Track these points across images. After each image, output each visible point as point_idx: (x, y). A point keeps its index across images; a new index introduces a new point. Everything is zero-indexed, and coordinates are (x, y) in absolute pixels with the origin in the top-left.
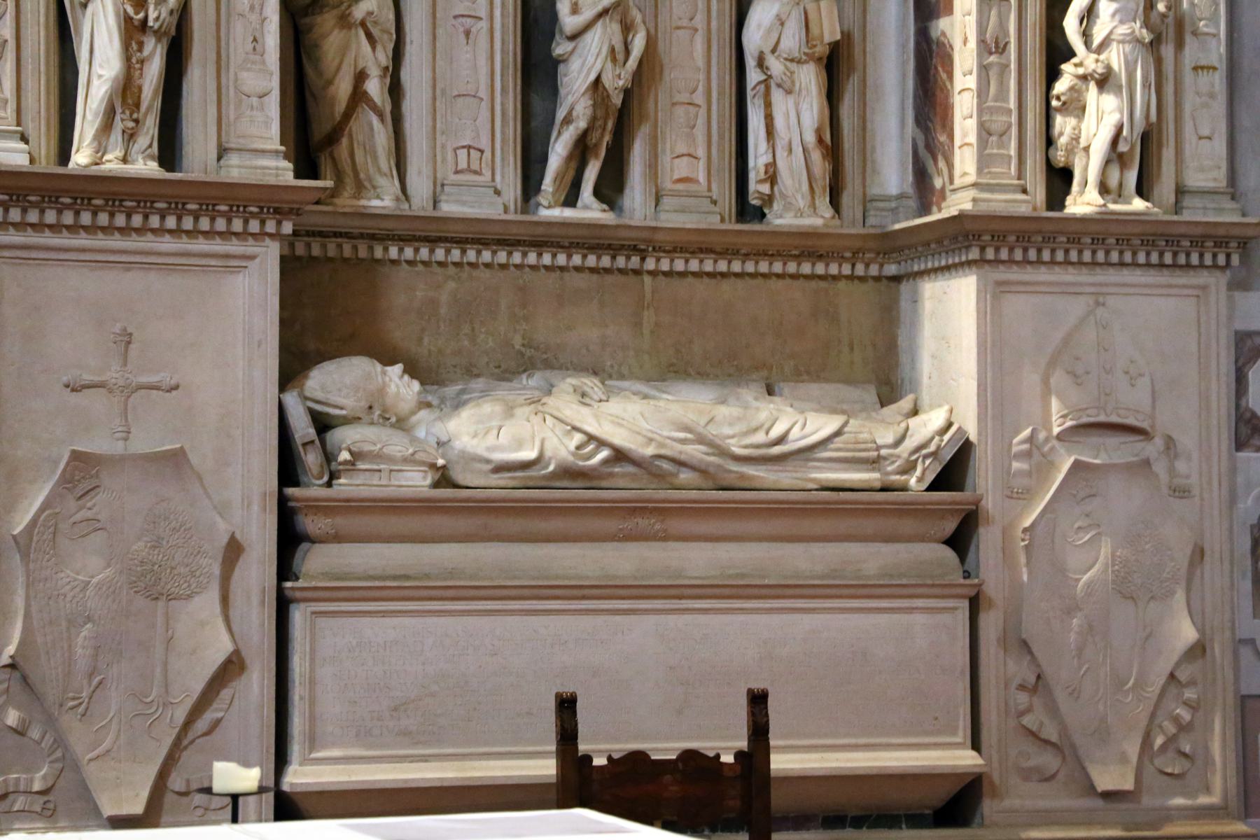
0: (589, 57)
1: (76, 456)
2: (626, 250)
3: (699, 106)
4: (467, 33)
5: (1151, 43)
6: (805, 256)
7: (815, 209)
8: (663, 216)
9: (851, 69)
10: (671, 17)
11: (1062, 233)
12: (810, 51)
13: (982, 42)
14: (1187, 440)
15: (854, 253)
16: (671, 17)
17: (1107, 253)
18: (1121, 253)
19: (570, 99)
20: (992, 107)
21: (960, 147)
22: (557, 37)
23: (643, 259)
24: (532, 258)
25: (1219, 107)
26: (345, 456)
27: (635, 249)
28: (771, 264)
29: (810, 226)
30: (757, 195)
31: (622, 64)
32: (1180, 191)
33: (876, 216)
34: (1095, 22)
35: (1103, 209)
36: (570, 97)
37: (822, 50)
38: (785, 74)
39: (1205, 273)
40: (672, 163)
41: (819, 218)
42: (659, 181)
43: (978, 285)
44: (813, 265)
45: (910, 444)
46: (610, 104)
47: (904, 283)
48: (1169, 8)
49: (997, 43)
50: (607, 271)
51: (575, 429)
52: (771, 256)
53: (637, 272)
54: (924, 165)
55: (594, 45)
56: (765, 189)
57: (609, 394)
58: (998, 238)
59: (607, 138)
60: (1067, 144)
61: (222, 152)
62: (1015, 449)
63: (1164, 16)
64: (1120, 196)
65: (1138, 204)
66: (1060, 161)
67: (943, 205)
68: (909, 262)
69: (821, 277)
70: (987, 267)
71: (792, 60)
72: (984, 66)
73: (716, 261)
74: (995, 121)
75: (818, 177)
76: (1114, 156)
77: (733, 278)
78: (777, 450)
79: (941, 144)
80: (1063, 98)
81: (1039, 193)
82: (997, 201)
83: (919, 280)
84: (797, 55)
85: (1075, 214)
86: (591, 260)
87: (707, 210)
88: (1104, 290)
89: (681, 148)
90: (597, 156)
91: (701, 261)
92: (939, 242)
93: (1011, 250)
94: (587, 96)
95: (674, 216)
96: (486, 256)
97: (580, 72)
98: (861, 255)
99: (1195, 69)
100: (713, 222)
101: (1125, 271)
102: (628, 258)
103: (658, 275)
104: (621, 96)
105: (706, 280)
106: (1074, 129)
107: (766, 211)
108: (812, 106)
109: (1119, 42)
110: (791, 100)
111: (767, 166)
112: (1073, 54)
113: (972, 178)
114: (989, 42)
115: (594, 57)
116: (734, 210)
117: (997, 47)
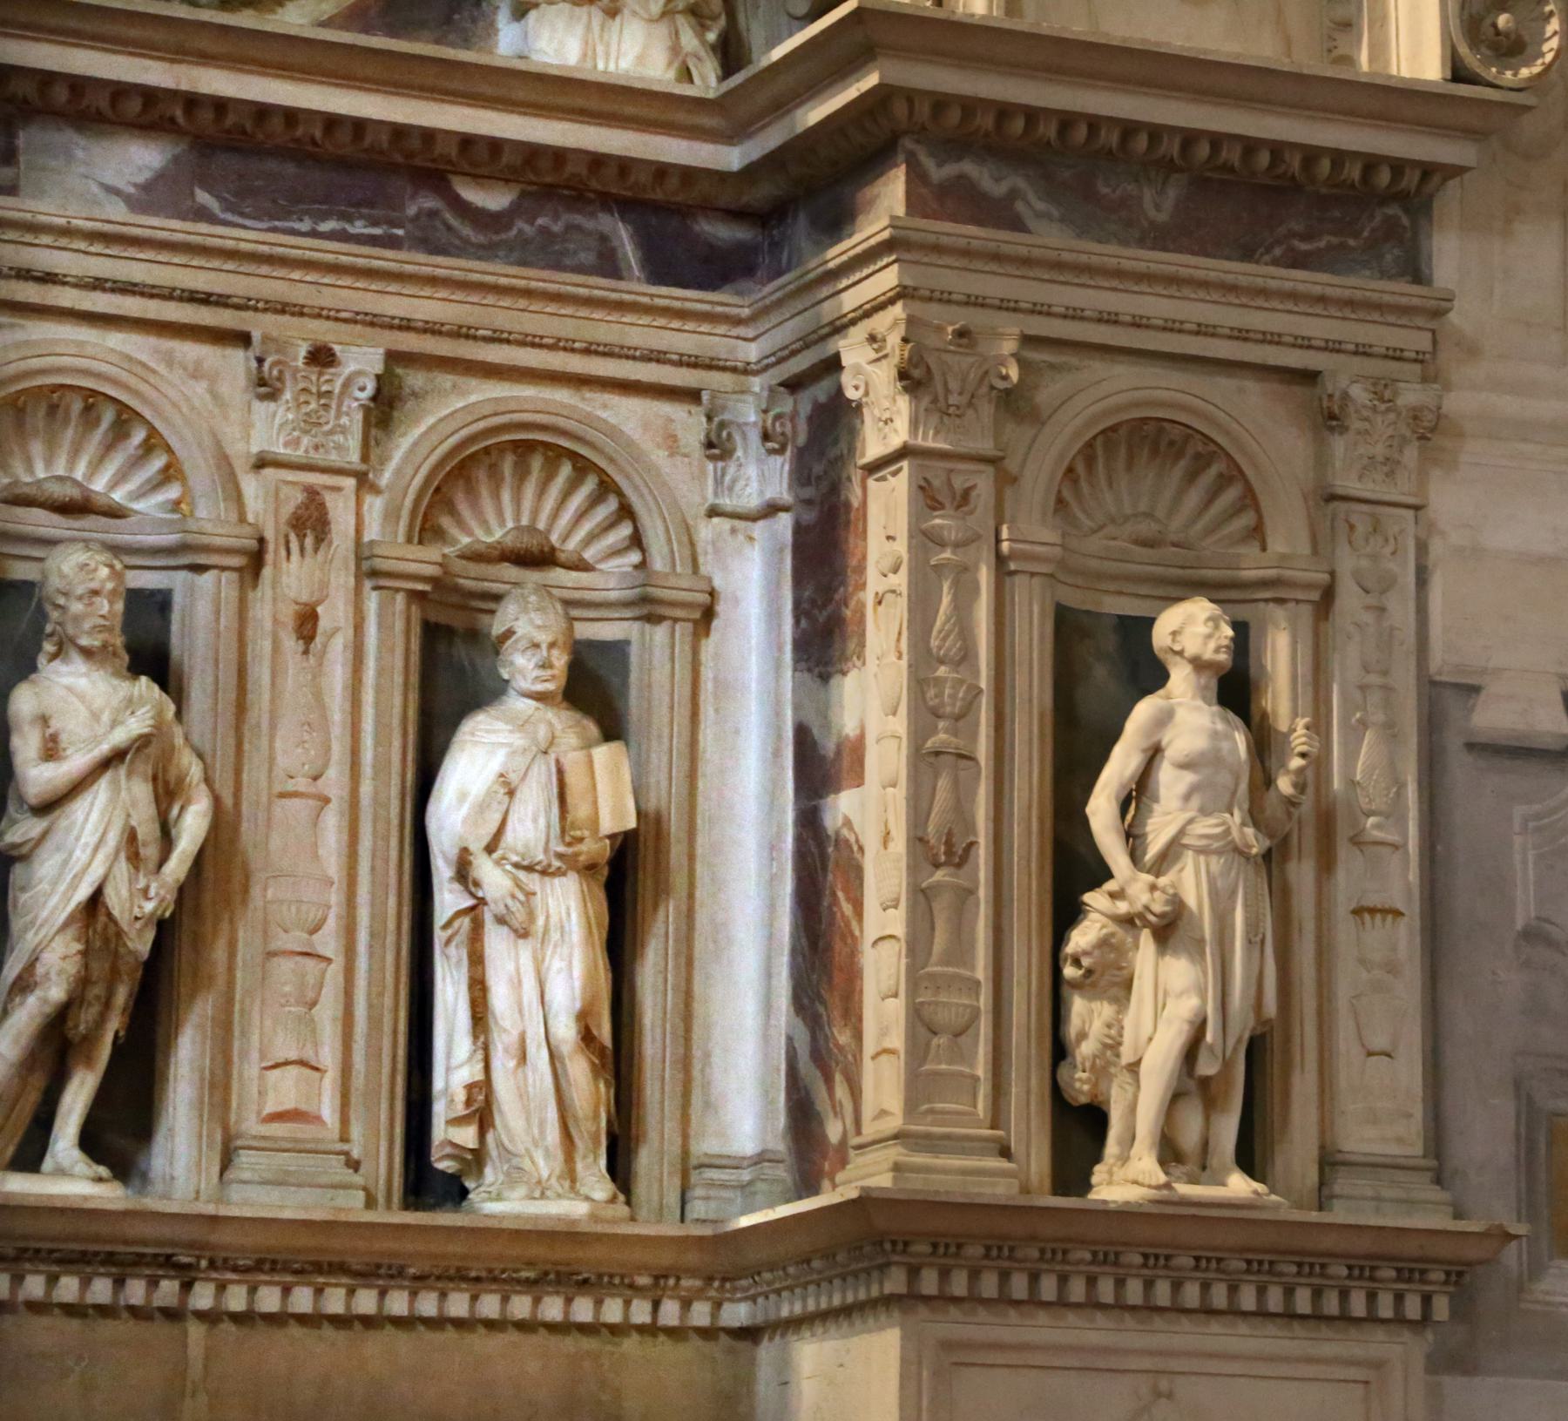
0: (78, 853)
2: (148, 1265)
3: (329, 960)
5: (1267, 856)
6: (550, 1283)
7: (573, 1180)
8: (236, 1193)
9: (662, 890)
10: (270, 770)
11: (1082, 1242)
12: (570, 850)
13: (917, 840)
15: (657, 1278)
16: (270, 770)
17: (1177, 1286)
18: (1206, 1287)
20: (943, 975)
21: (873, 1058)
22: (11, 808)
23: (187, 1286)
25: (1408, 990)
27: (168, 1263)
28: (474, 1298)
29: (559, 1219)
30: (448, 1150)
31: (152, 865)
32: (1329, 1161)
33: (707, 1198)
34: (1151, 811)
35: (1165, 1192)
36: (30, 935)
37: (595, 849)
38: (513, 897)
40: (261, 1078)
42: (233, 1118)
43: (903, 1348)
44: (569, 1301)
46: (122, 950)
47: (765, 1342)
48: (1300, 787)
49: (949, 844)
50: (104, 1311)
52: (476, 1283)
53: (173, 1315)
54: (808, 1093)
55: (89, 826)
56: (467, 1136)
58: (947, 1249)
59: (114, 1024)
60: (1095, 1057)
63: (1291, 803)
64: (1204, 1168)
65: (1239, 1185)
66: (1081, 1092)
67: (840, 1177)
68: (773, 1297)
69: (583, 1328)
70: (923, 1311)
71: (529, 869)
72: (923, 891)
73: (351, 1292)
74: (945, 1004)
75: (580, 1114)
76: (1192, 1085)
77: (389, 1329)
79: (841, 1048)
80: (1086, 962)
81: (1037, 1159)
82: (945, 1171)
83: (791, 1337)
84: (541, 857)
85: (1105, 1202)
87: (337, 1179)
88: (1174, 1364)
89: (286, 1048)
90: (89, 1062)
91: (319, 1291)
92: (829, 1255)
93: (975, 1274)
94: (71, 932)
95: (254, 1193)
97: (55, 883)
98: (671, 1282)
99: (1358, 912)
100: (352, 1206)
101: (1215, 1326)
102: (153, 1283)
103: (222, 1320)
104: (150, 935)
105: (328, 1331)
106: (1109, 1026)
107: (469, 1184)
108: (570, 963)
109: (1200, 851)
110: (525, 951)
111: (470, 1088)
112: (1108, 875)
113: (895, 1123)
114: (933, 841)
115: (89, 851)
116: (397, 1181)
117: (949, 852)
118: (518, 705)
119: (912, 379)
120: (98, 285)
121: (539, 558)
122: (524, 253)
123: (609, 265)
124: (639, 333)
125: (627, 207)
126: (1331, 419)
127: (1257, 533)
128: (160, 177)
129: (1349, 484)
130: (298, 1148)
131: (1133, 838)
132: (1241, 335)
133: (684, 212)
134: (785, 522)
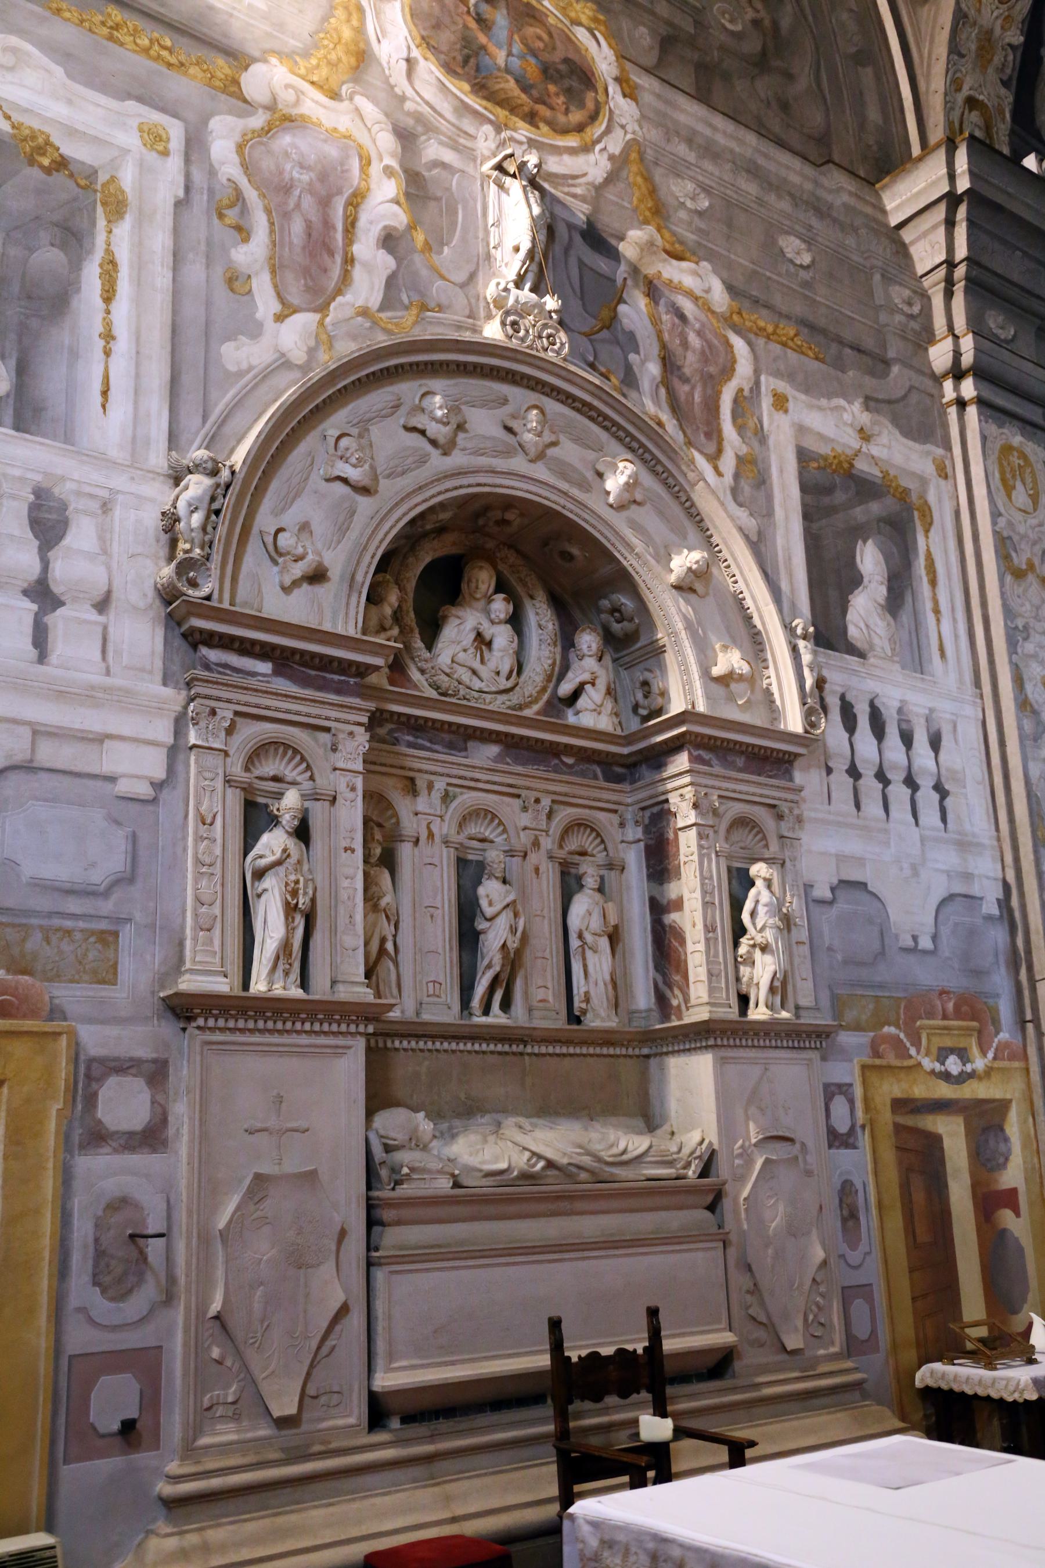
1: (258, 1177)
4: (432, 916)
13: (705, 926)
14: (810, 1145)
19: (491, 954)
24: (469, 1046)
26: (405, 1170)
32: (797, 1008)
37: (611, 929)
39: (810, 1052)
41: (612, 1023)
45: (686, 1151)
50: (506, 1053)
51: (525, 1149)
53: (521, 1054)
57: (535, 1126)
61: (334, 983)
62: (736, 1152)
78: (625, 1157)
81: (736, 1009)
86: (499, 1048)
89: (540, 983)
96: (446, 1045)
118: (587, 891)
119: (695, 806)
120: (488, 782)
121: (583, 854)
122: (576, 774)
123: (596, 778)
124: (606, 795)
125: (599, 763)
126: (780, 817)
127: (767, 846)
128: (499, 755)
129: (786, 834)
130: (546, 1009)
131: (754, 924)
132: (761, 796)
133: (611, 764)
134: (642, 844)
